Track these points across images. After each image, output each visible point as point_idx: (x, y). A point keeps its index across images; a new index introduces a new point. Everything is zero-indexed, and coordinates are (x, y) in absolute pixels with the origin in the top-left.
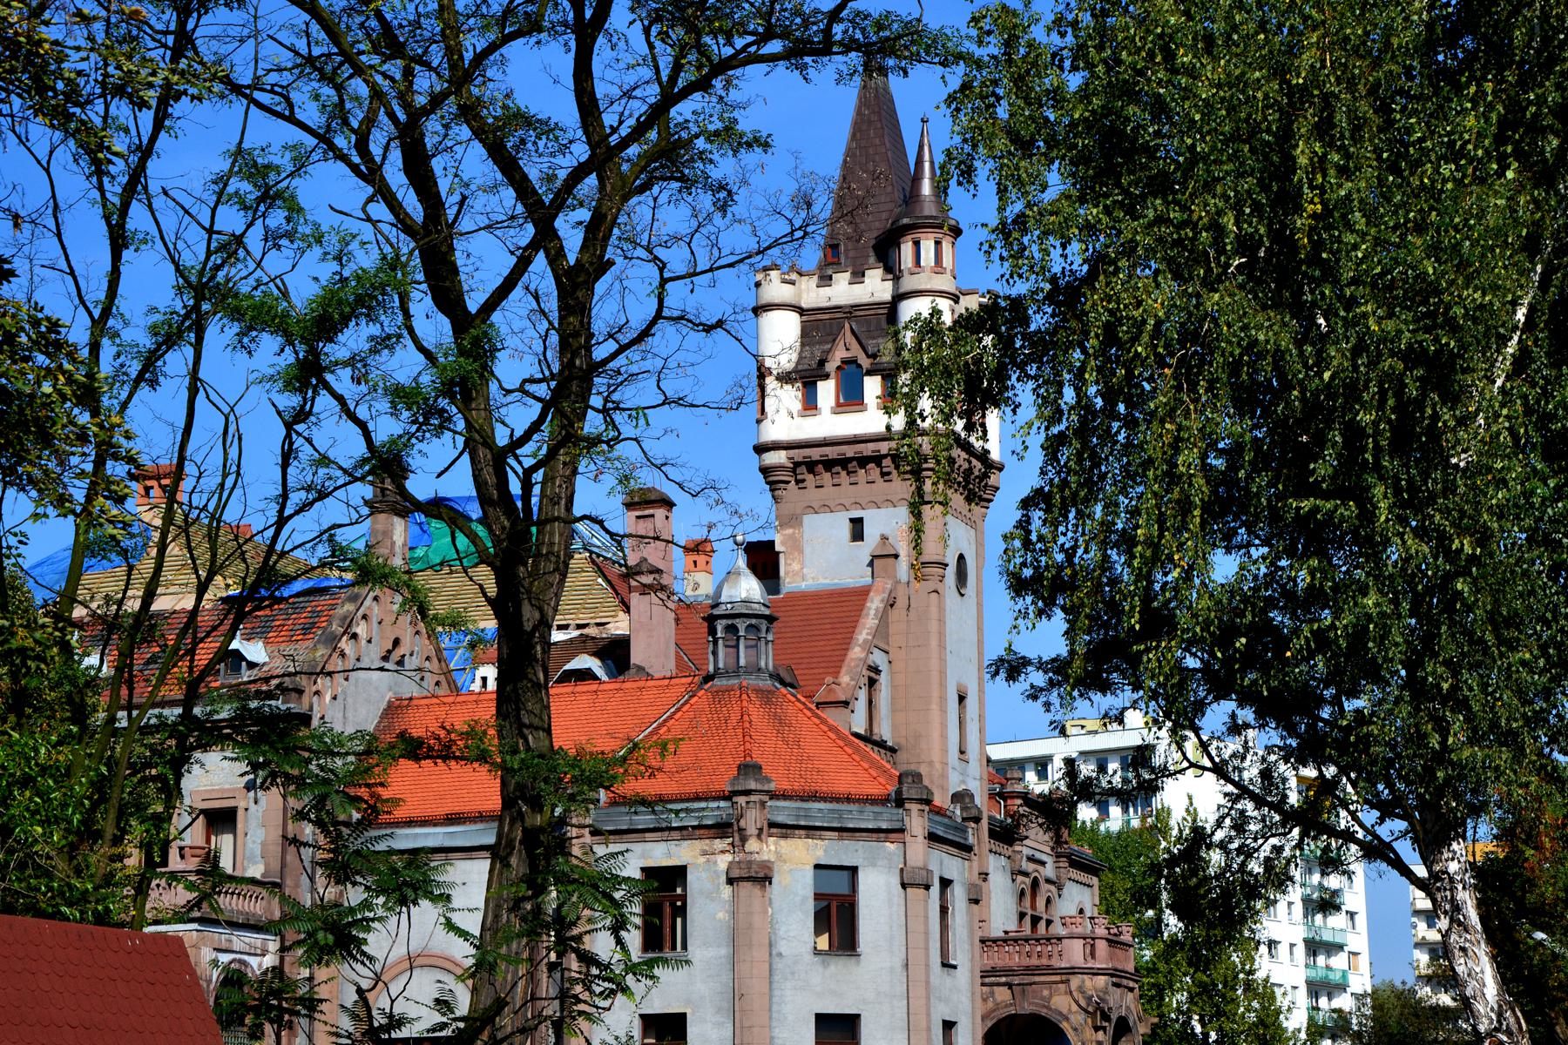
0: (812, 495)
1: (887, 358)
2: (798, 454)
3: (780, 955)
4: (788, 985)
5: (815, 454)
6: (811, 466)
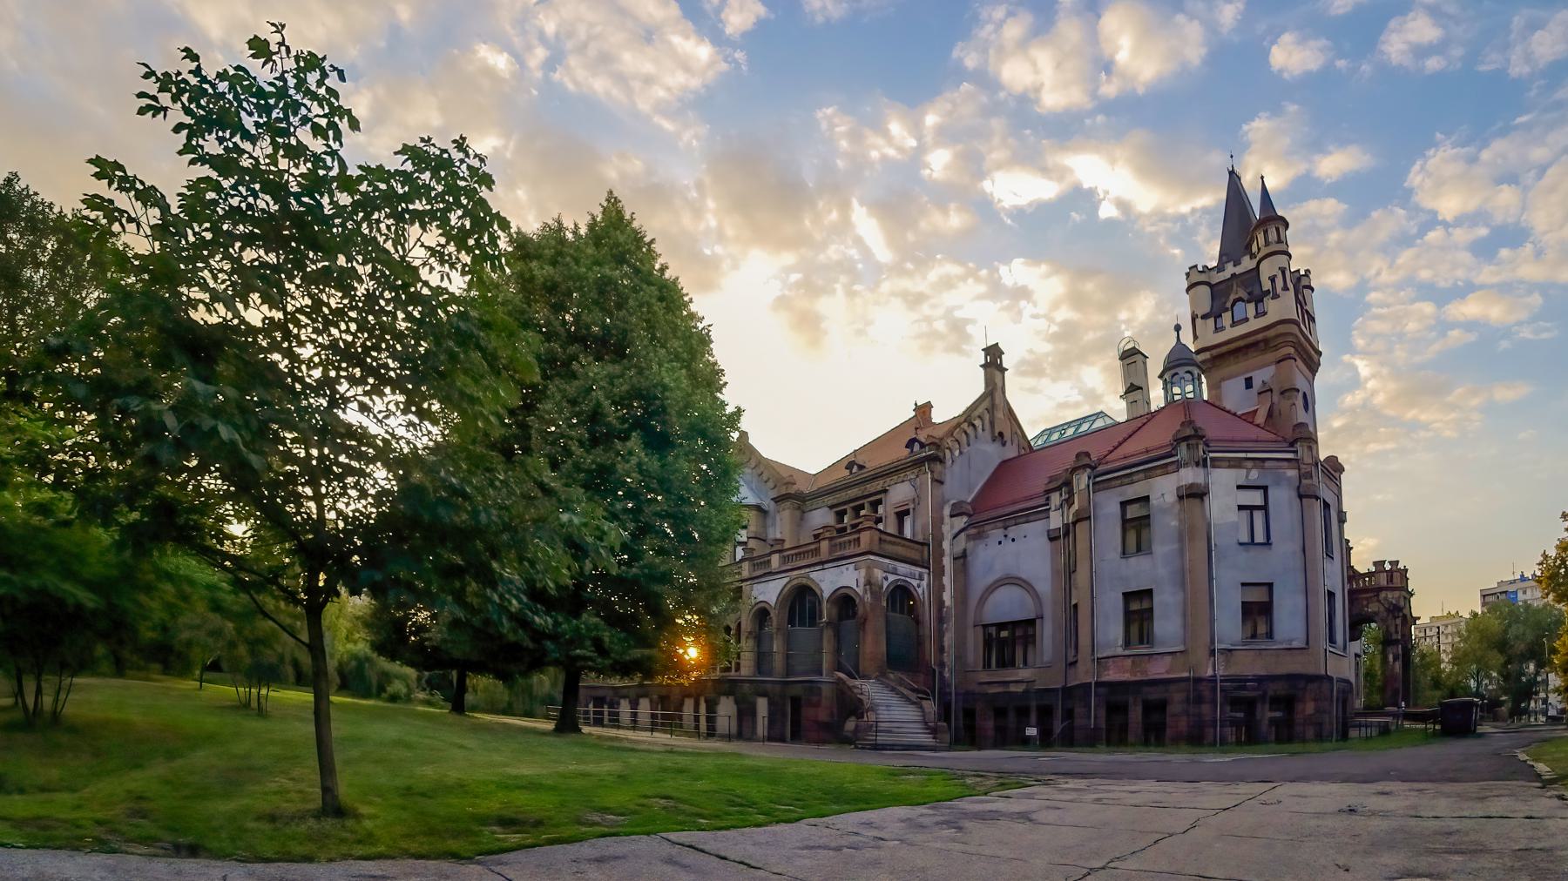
0: (1225, 371)
1: (1257, 292)
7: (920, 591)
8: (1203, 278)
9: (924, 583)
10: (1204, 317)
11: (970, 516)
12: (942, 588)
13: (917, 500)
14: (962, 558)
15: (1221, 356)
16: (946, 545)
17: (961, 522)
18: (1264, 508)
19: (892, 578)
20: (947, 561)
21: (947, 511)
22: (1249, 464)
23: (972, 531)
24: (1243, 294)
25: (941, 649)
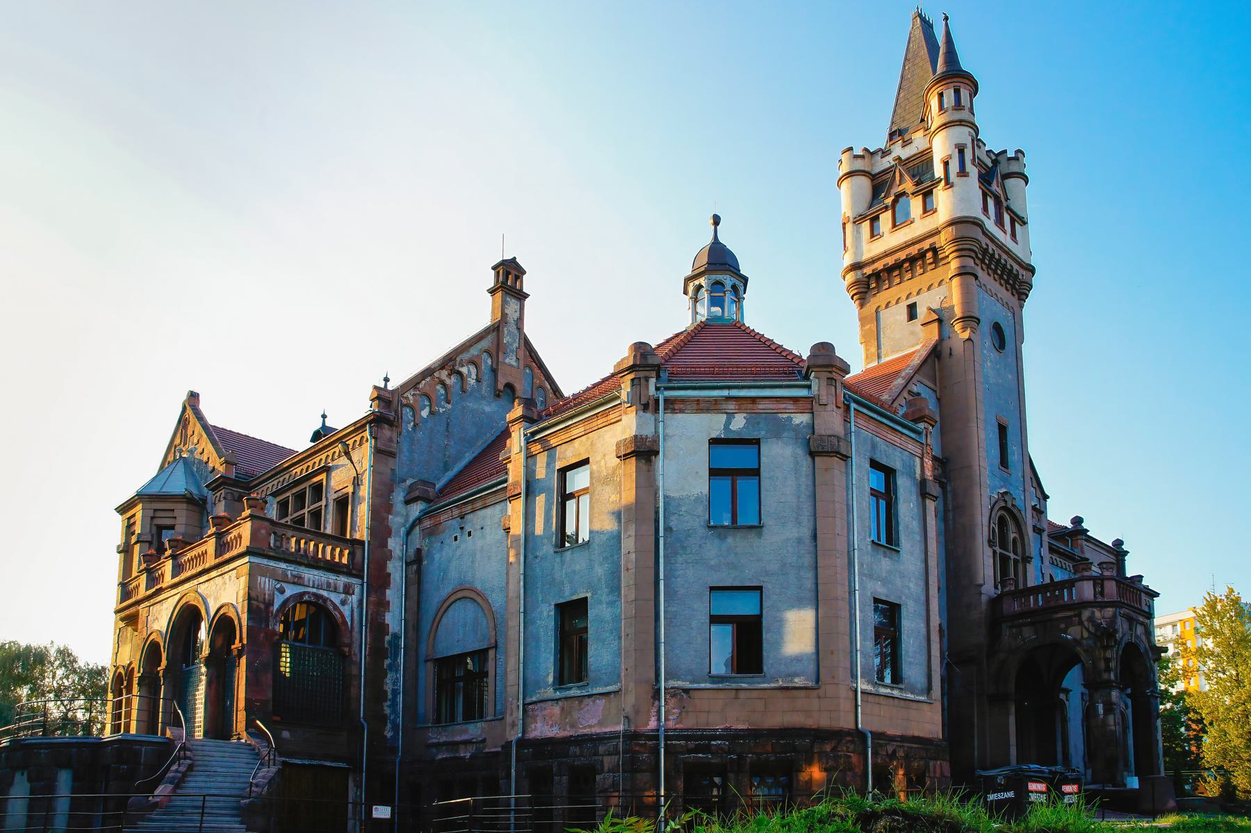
2: (868, 271)
4: (680, 559)
5: (879, 266)
6: (877, 275)
7: (346, 611)
9: (354, 599)
10: (858, 220)
11: (427, 500)
12: (383, 605)
13: (357, 482)
14: (416, 562)
16: (394, 544)
17: (417, 509)
18: (756, 473)
19: (290, 590)
20: (395, 569)
21: (399, 496)
22: (731, 406)
23: (427, 523)
24: (908, 186)
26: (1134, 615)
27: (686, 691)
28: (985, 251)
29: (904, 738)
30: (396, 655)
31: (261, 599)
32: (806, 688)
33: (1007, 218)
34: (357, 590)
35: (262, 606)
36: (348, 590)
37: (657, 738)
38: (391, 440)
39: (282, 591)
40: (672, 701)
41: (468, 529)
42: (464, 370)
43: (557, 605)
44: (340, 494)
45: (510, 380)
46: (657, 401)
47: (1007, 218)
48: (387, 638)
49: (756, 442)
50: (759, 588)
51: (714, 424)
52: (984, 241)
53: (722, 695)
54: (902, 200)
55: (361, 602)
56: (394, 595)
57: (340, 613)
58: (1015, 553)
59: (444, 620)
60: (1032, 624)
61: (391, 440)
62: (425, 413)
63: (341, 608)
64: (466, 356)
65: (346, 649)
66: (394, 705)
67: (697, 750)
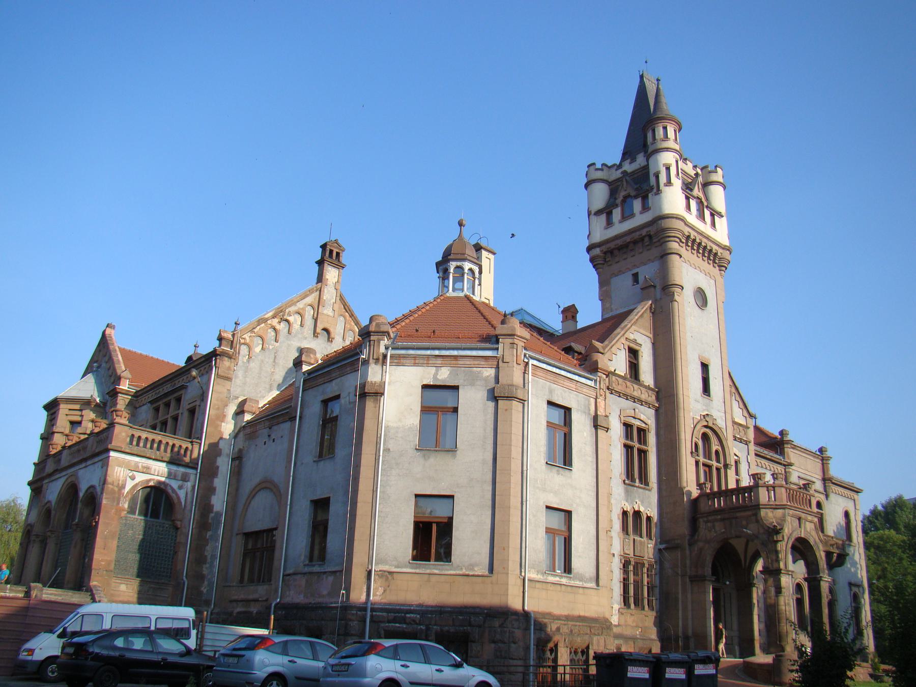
3: (387, 450)
7: (182, 494)
8: (599, 175)
9: (189, 485)
10: (598, 213)
12: (211, 490)
15: (611, 252)
18: (455, 410)
19: (140, 478)
22: (439, 361)
25: (199, 559)
26: (803, 515)
27: (391, 573)
28: (688, 237)
29: (568, 618)
30: (218, 528)
31: (116, 484)
32: (482, 576)
33: (707, 213)
34: (192, 477)
35: (116, 489)
36: (185, 478)
37: (365, 609)
38: (229, 368)
39: (133, 478)
40: (380, 582)
41: (273, 437)
42: (291, 319)
43: (312, 501)
44: (191, 405)
45: (327, 326)
46: (385, 356)
47: (707, 213)
48: (212, 515)
49: (456, 388)
50: (452, 497)
51: (428, 375)
52: (687, 230)
53: (416, 577)
54: (629, 200)
55: (194, 487)
56: (221, 483)
57: (177, 494)
58: (718, 461)
59: (252, 503)
60: (723, 520)
61: (229, 368)
62: (258, 349)
63: (179, 492)
64: (293, 309)
65: (178, 523)
66: (212, 566)
67: (394, 620)
